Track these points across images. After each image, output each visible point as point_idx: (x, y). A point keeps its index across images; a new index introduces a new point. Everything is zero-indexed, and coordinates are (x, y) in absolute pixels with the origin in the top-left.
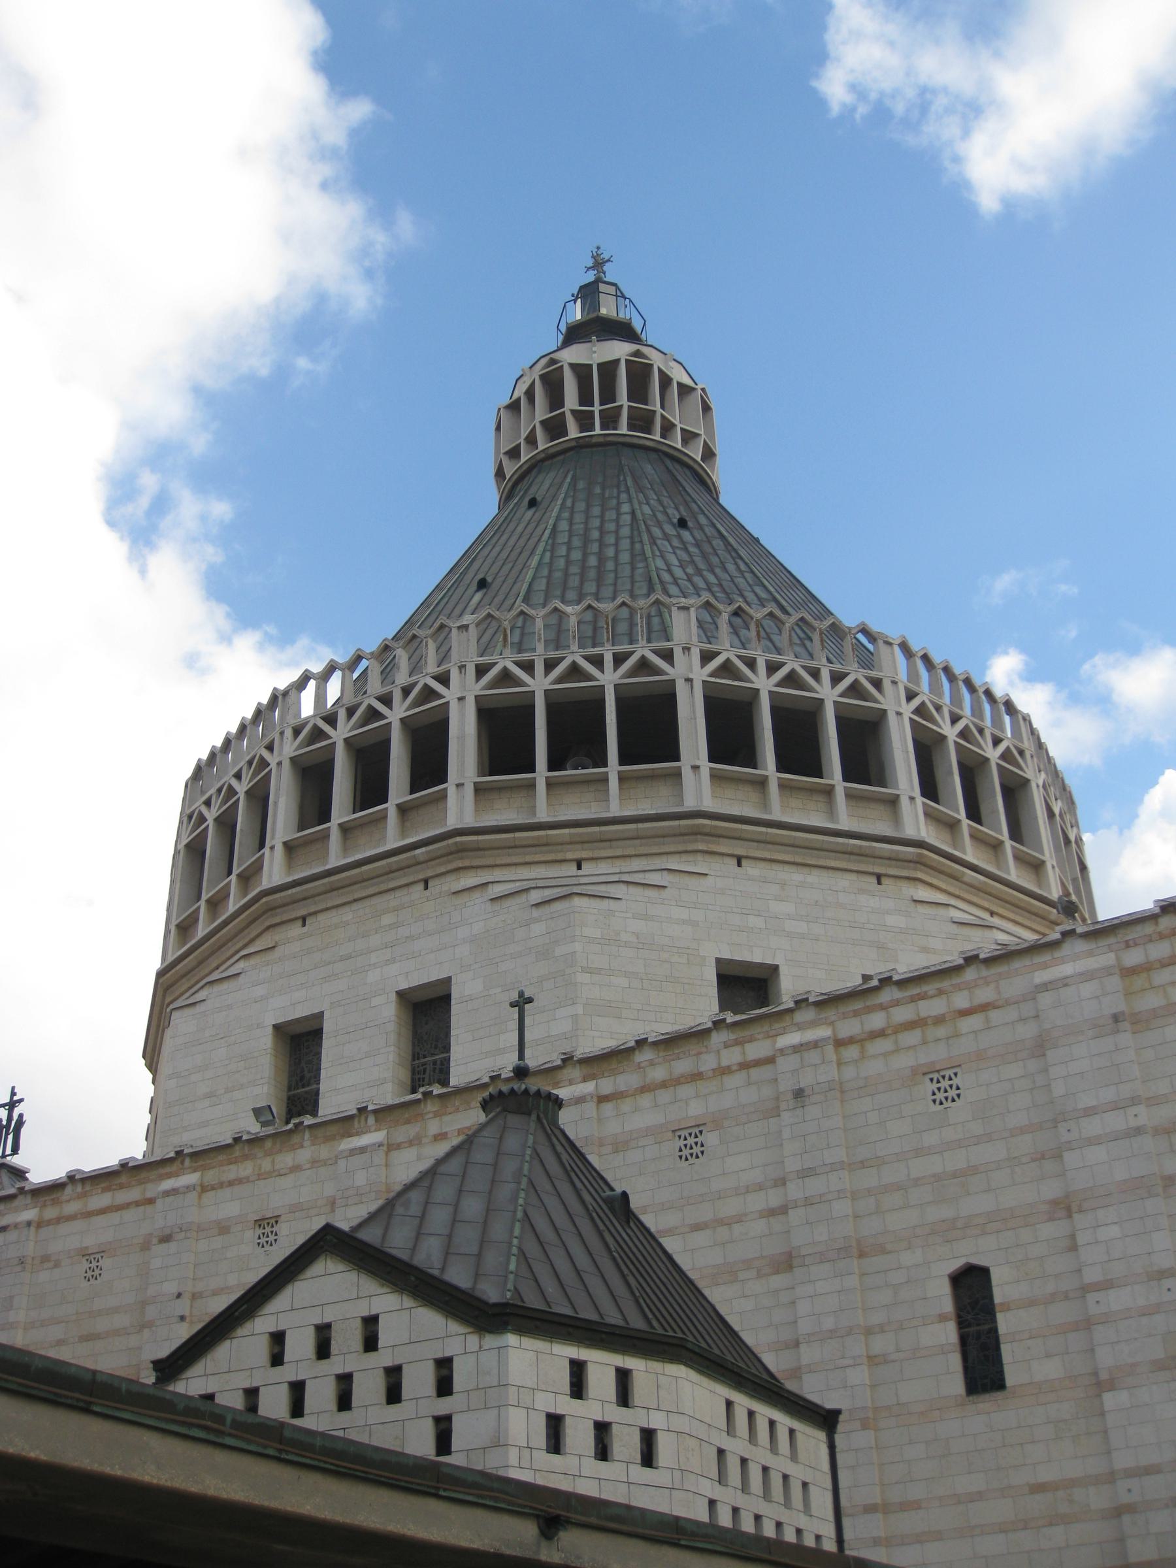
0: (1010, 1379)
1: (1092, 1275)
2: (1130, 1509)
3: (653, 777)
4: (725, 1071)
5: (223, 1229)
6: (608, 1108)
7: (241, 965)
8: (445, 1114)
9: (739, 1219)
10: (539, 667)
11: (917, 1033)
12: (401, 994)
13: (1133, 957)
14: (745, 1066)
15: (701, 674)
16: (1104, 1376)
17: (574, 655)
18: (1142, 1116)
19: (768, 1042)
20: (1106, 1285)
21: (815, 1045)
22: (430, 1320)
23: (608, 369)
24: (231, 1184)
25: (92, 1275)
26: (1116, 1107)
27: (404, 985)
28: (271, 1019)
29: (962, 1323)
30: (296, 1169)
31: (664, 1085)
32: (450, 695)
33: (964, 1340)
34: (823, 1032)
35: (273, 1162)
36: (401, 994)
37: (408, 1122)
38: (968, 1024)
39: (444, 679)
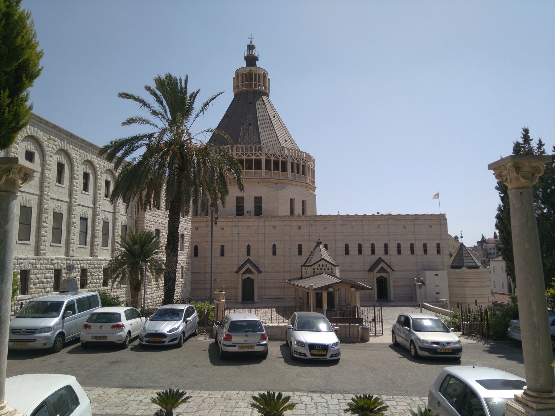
1: (337, 247)
4: (304, 221)
5: (242, 226)
6: (291, 222)
10: (273, 156)
13: (344, 219)
14: (306, 221)
20: (337, 248)
21: (314, 220)
22: (331, 265)
23: (259, 75)
28: (236, 196)
30: (252, 221)
31: (297, 221)
32: (262, 157)
34: (314, 220)
38: (328, 222)
39: (261, 154)
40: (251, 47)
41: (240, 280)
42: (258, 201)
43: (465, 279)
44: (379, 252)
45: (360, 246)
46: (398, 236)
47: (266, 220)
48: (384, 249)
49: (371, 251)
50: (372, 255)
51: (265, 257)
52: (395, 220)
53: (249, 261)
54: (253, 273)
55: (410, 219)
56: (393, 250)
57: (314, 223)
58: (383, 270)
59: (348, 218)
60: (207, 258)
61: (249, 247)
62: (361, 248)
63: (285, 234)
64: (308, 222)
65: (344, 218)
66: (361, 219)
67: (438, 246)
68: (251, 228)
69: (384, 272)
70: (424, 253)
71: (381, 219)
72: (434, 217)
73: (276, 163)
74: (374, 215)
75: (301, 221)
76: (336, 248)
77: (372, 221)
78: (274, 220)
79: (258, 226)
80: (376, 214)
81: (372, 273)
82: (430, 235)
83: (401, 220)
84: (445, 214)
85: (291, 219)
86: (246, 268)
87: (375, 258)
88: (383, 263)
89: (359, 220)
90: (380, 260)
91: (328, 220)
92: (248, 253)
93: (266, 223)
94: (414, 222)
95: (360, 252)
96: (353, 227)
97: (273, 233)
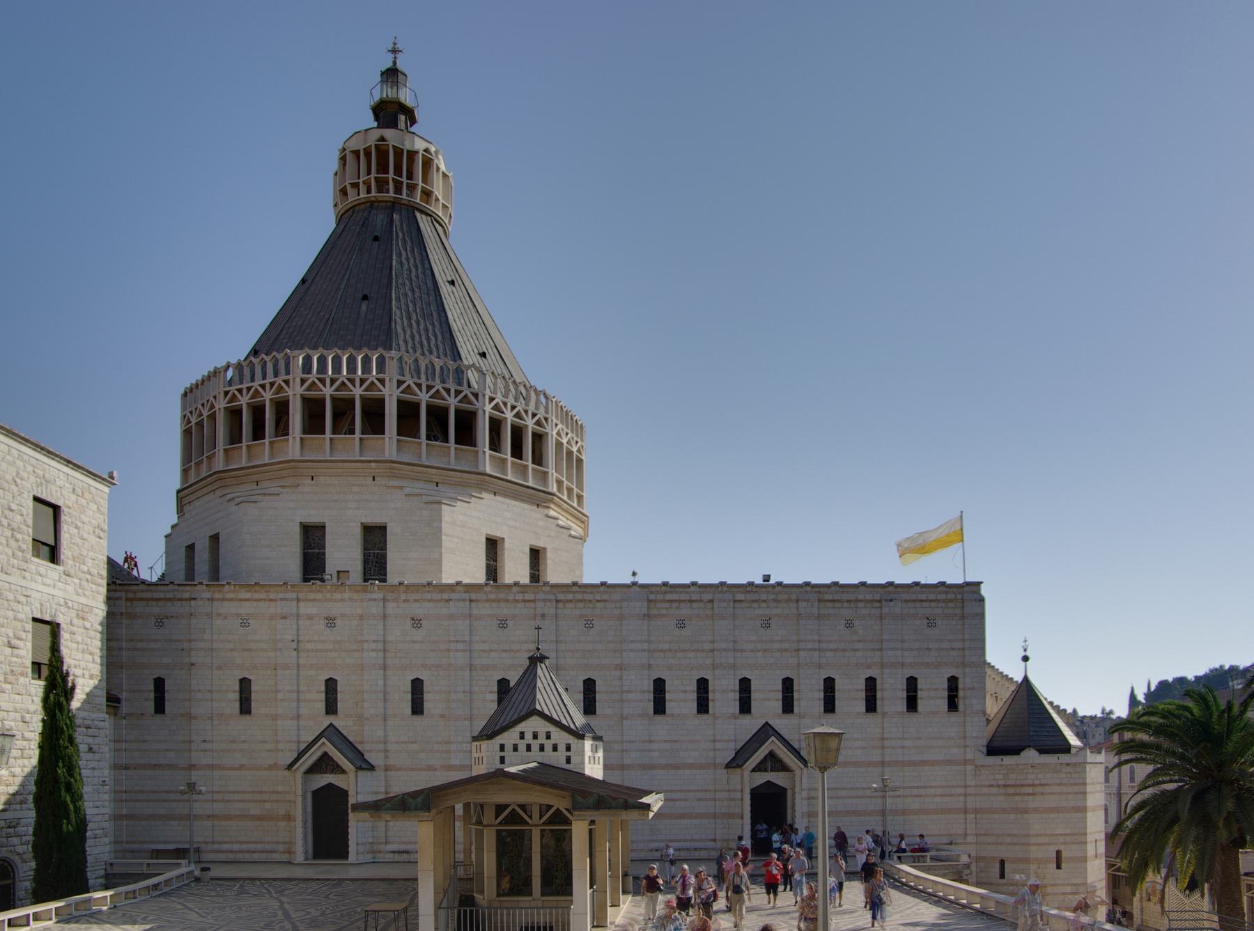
0: (597, 713)
1: (625, 688)
2: (627, 751)
3: (467, 450)
4: (517, 601)
5: (310, 618)
6: (473, 604)
7: (278, 490)
8: (408, 592)
9: (519, 651)
11: (583, 604)
12: (362, 523)
13: (652, 597)
14: (524, 601)
15: (488, 408)
16: (624, 716)
17: (439, 386)
18: (646, 646)
19: (533, 595)
20: (629, 692)
21: (550, 600)
24: (312, 600)
25: (245, 624)
26: (640, 642)
27: (364, 521)
28: (298, 520)
29: (585, 694)
30: (342, 600)
31: (494, 601)
33: (584, 698)
35: (332, 596)
36: (362, 523)
37: (392, 592)
38: (599, 605)
40: (392, 75)
41: (299, 792)
42: (374, 536)
43: (1029, 785)
44: (767, 705)
45: (703, 685)
46: (829, 654)
47: (389, 596)
48: (780, 695)
49: (738, 703)
50: (742, 716)
51: (385, 720)
52: (820, 601)
53: (331, 733)
54: (343, 772)
55: (869, 597)
56: (809, 696)
57: (550, 610)
58: (773, 763)
59: (665, 592)
60: (195, 718)
61: (331, 685)
62: (707, 692)
63: (453, 646)
64: (532, 605)
65: (651, 592)
66: (707, 597)
67: (953, 684)
68: (338, 622)
69: (778, 770)
70: (908, 708)
71: (773, 597)
72: (946, 593)
73: (438, 416)
74: (751, 584)
75: (508, 601)
76: (622, 692)
77: (743, 605)
78: (418, 596)
79: (361, 617)
80: (759, 581)
81: (738, 771)
82: (930, 649)
83: (838, 601)
84: (979, 584)
85: (473, 596)
86: (319, 754)
87: (750, 725)
88: (773, 738)
89: (701, 601)
90: (766, 731)
91: (598, 601)
92: (331, 708)
93: (391, 608)
94: (881, 608)
95: (703, 706)
96: (681, 624)
97: (412, 642)
